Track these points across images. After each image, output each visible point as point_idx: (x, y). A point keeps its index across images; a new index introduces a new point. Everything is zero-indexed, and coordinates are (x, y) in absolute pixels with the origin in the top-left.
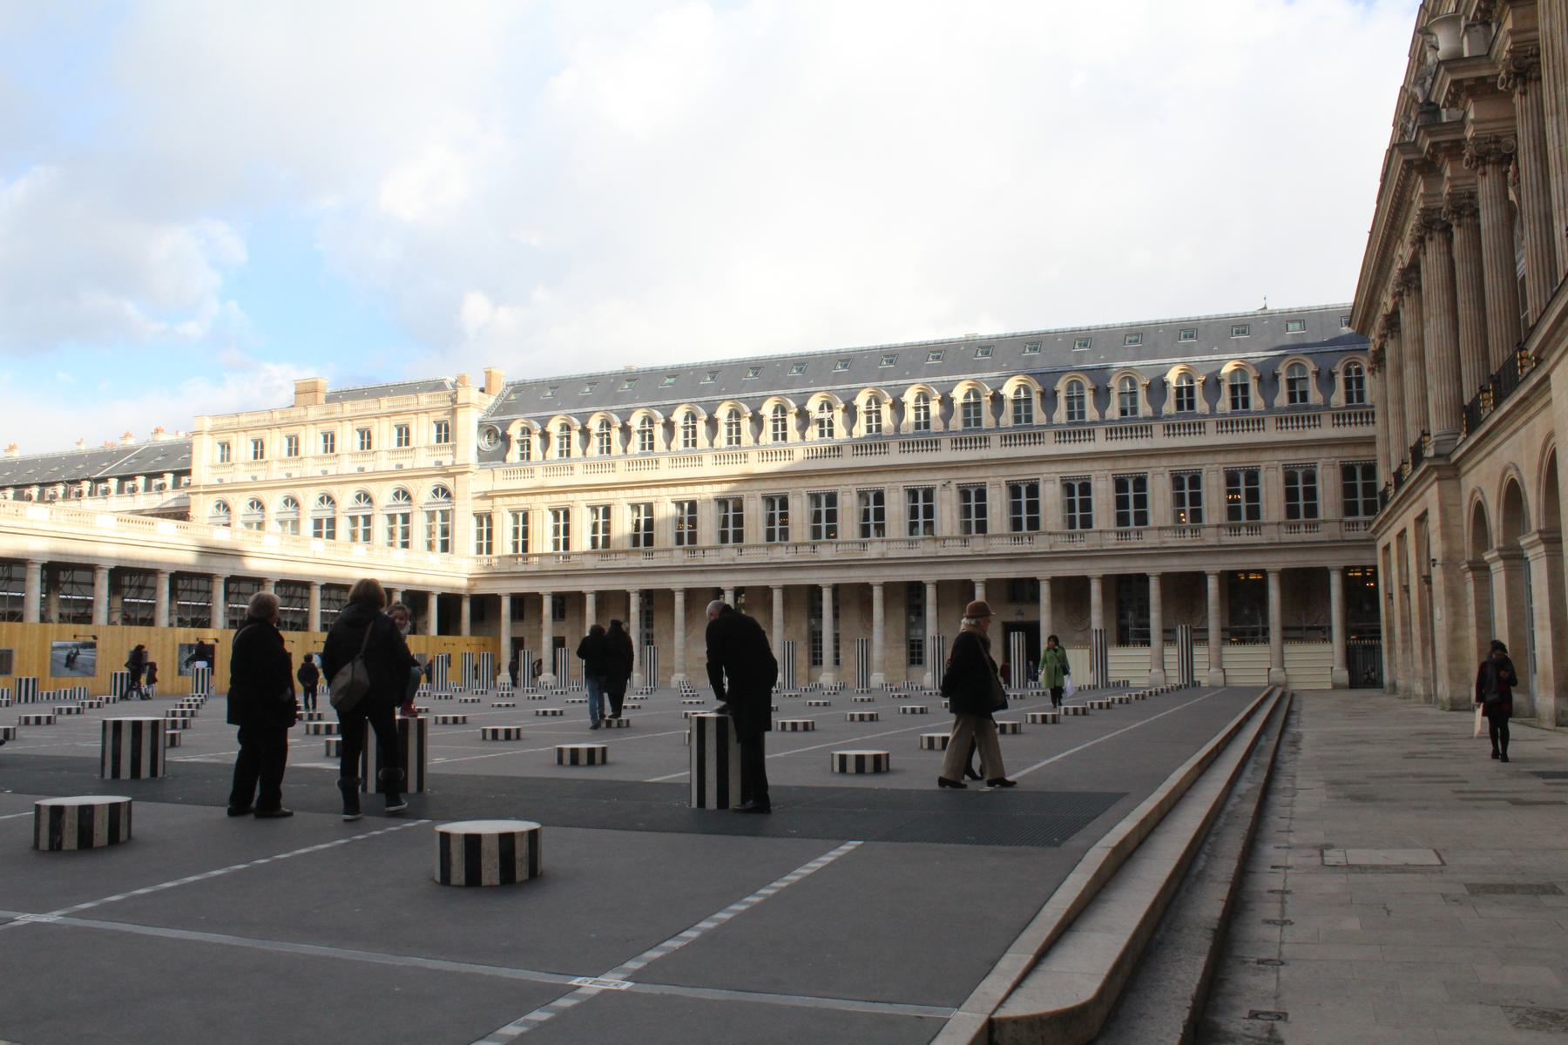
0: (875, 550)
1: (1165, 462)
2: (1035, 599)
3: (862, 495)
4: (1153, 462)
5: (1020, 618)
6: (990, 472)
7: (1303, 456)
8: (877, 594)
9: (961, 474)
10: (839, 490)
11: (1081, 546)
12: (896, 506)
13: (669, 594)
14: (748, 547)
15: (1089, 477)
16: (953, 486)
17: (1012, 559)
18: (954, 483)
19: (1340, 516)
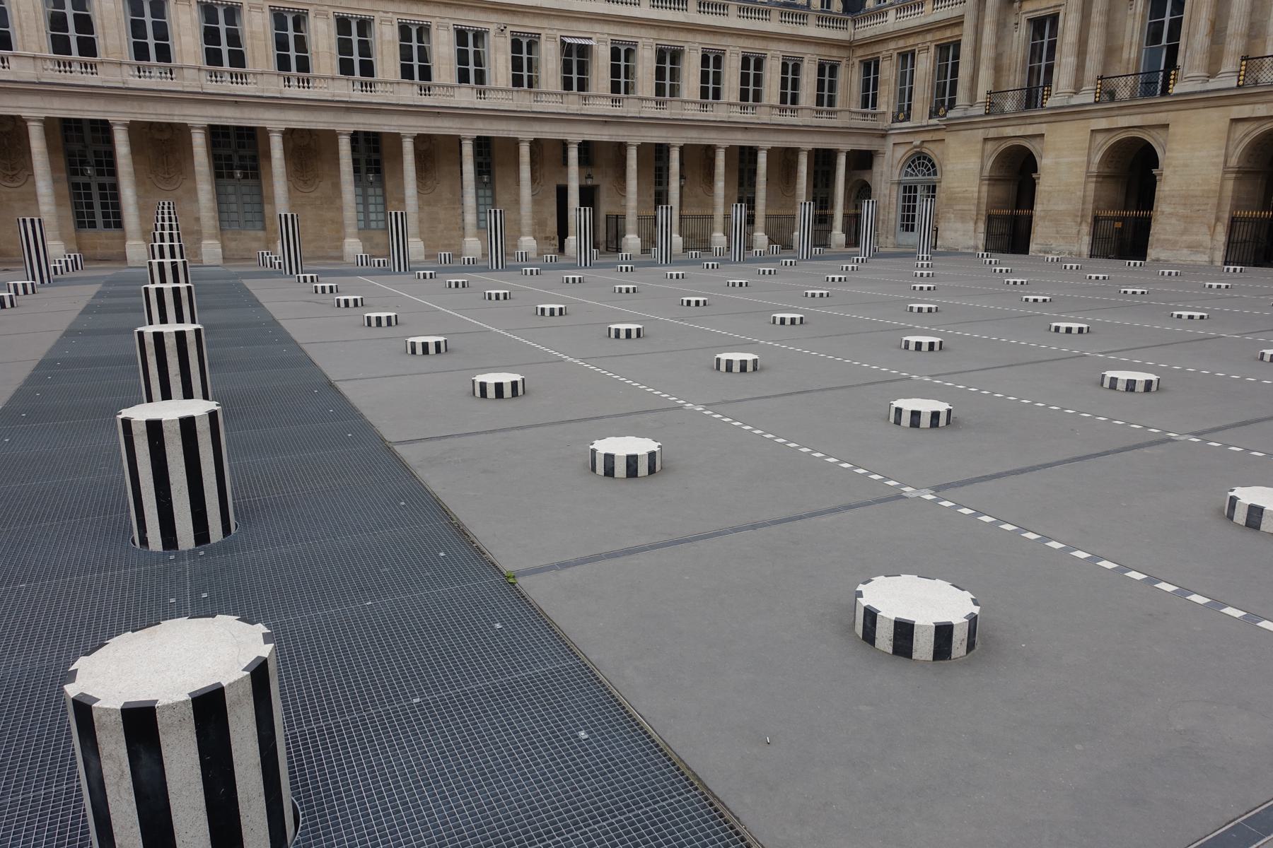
1: (700, 38)
2: (565, 162)
4: (690, 37)
5: (589, 182)
6: (544, 23)
7: (796, 50)
9: (516, 20)
11: (665, 114)
12: (443, 49)
14: (435, 86)
16: (508, 34)
17: (606, 121)
18: (510, 29)
19: (609, 93)
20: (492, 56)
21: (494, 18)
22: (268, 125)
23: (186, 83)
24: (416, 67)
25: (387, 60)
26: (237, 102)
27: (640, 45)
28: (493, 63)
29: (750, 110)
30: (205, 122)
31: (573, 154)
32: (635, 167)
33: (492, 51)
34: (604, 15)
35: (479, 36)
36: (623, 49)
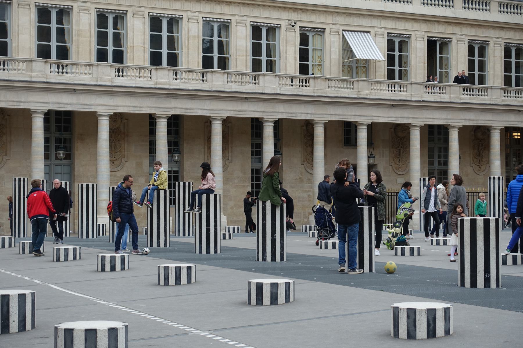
0: (268, 84)
3: (208, 24)
4: (457, 30)
6: (330, 19)
8: (319, 132)
9: (305, 17)
10: (185, 15)
12: (240, 42)
13: (92, 118)
15: (409, 36)
20: (283, 48)
21: (286, 15)
22: (99, 110)
23: (33, 74)
24: (215, 57)
25: (191, 55)
26: (75, 90)
27: (413, 38)
28: (283, 55)
29: (513, 94)
30: (46, 108)
31: (362, 135)
32: (418, 146)
33: (283, 44)
34: (382, 11)
35: (272, 30)
36: (397, 41)
